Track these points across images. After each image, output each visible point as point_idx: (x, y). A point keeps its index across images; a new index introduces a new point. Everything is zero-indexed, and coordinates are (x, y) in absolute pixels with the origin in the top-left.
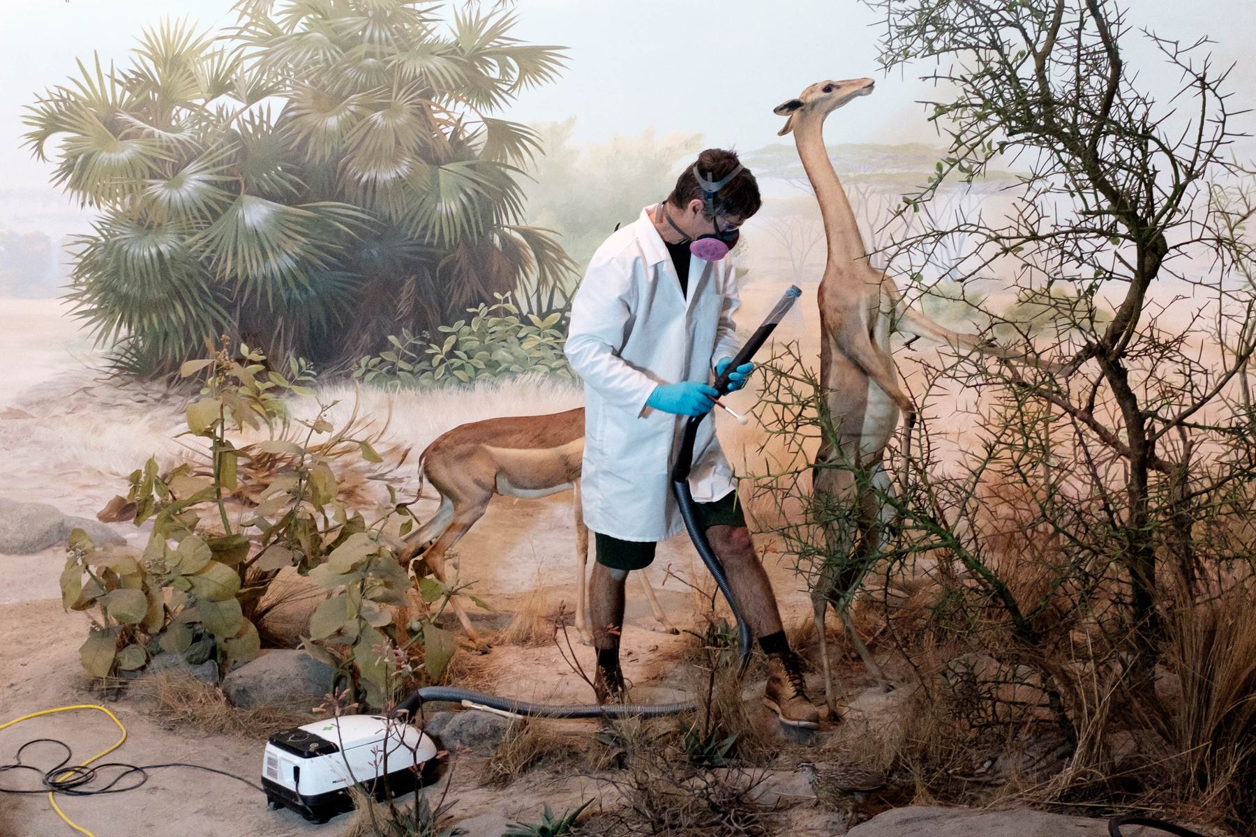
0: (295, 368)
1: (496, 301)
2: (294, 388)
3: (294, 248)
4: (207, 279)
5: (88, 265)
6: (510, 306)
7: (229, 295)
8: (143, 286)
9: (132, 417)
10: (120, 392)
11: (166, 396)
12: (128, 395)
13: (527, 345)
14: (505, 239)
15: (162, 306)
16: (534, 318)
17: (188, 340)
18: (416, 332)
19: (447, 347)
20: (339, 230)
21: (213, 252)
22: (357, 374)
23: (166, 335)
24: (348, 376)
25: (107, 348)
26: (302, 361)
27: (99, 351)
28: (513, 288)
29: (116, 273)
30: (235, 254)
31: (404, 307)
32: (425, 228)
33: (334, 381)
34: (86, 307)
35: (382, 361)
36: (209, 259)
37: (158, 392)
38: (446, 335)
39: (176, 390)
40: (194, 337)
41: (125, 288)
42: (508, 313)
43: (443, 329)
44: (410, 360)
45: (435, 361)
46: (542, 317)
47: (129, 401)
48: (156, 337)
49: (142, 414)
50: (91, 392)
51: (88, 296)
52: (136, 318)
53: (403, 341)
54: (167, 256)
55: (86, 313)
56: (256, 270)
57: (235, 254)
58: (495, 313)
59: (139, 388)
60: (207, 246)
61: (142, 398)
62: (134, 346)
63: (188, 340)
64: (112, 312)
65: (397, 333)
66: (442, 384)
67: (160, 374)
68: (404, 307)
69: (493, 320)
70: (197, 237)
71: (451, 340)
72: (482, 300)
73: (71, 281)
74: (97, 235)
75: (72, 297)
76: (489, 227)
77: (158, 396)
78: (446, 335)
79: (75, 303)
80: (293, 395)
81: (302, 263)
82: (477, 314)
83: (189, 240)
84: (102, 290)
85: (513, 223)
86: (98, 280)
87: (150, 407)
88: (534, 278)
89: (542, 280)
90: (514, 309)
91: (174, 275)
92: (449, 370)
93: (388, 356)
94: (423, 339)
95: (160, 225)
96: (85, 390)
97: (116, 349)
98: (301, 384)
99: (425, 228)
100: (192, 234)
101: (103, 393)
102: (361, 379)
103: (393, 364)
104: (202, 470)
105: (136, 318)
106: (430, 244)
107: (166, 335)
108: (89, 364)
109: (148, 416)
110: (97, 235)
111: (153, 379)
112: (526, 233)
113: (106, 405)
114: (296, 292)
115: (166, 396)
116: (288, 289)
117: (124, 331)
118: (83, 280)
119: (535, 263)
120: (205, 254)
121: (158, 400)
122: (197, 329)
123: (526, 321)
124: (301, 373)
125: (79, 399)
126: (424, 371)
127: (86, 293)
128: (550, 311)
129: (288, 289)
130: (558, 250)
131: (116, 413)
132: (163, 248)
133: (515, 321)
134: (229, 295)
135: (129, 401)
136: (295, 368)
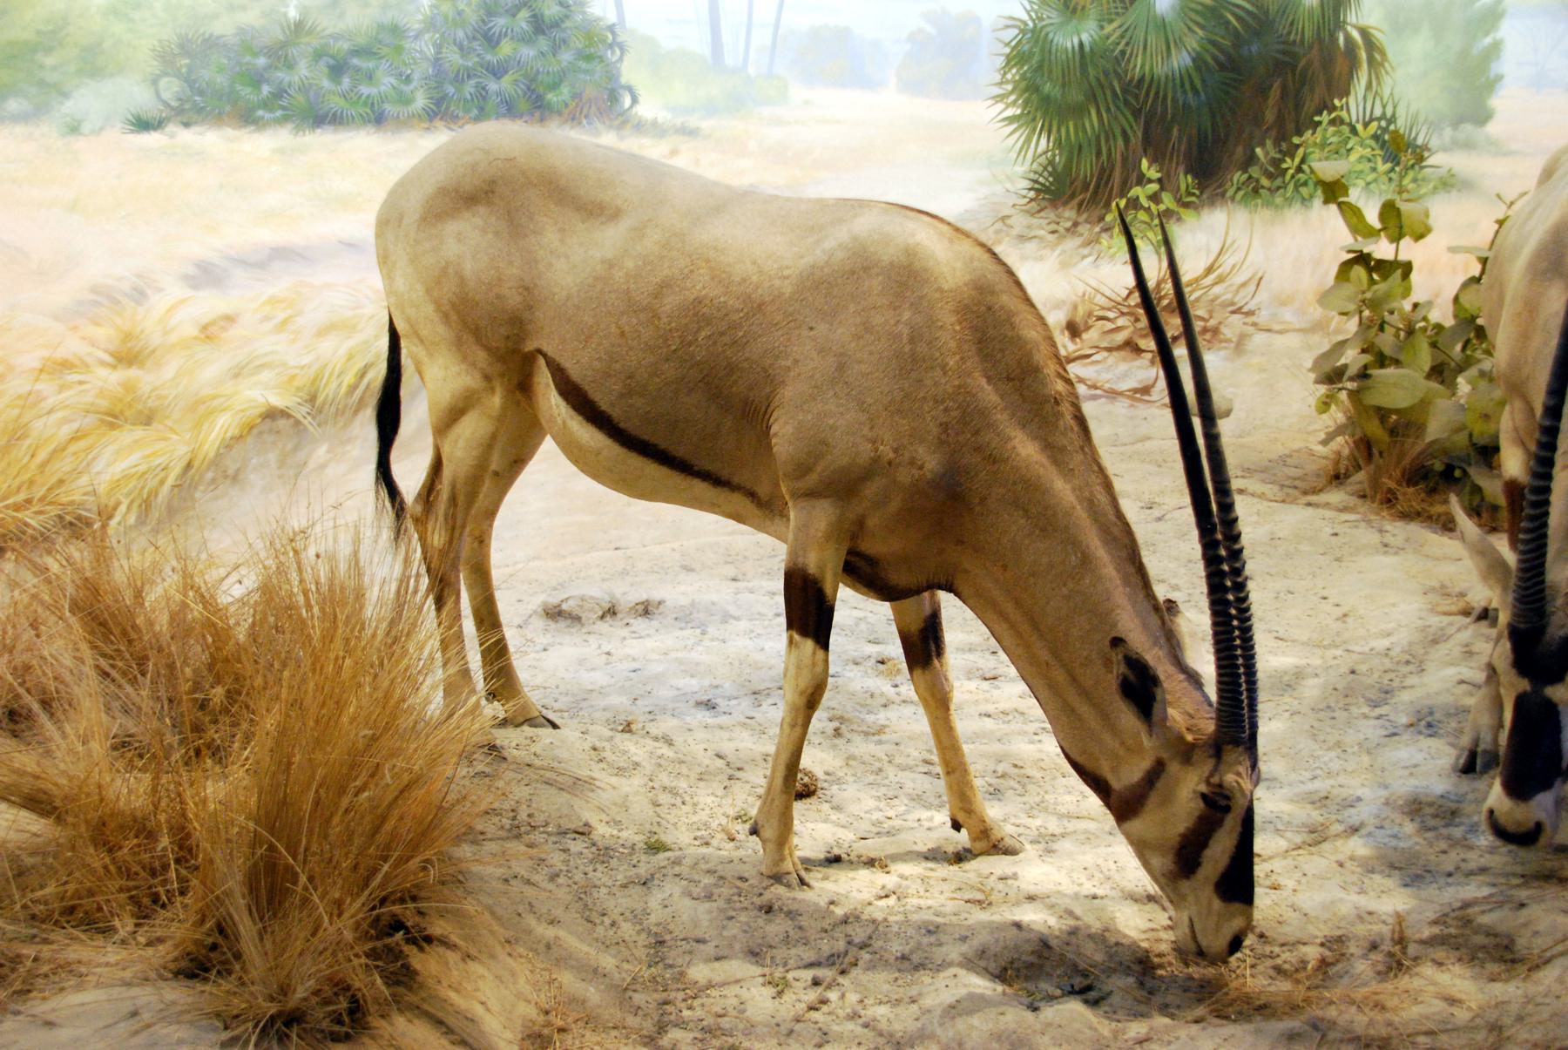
0: (1183, 187)
1: (1335, 108)
2: (1181, 210)
3: (1192, 43)
4: (1120, 78)
5: (1017, 57)
6: (1344, 114)
7: (1136, 97)
8: (1063, 85)
9: (1044, 252)
10: (1035, 221)
11: (1076, 224)
12: (1040, 225)
13: (1353, 157)
14: (1348, 38)
15: (1078, 111)
16: (1359, 127)
17: (1099, 153)
18: (1277, 143)
19: (1297, 160)
20: (1228, 22)
21: (1127, 44)
22: (1229, 194)
23: (1080, 147)
24: (1223, 195)
25: (1026, 167)
26: (1189, 178)
27: (1020, 169)
28: (1347, 93)
29: (1040, 67)
30: (1145, 48)
31: (1270, 116)
32: (1292, 24)
33: (1212, 203)
34: (1010, 112)
35: (1250, 177)
36: (1123, 53)
37: (1068, 219)
38: (1298, 146)
39: (1085, 216)
40: (1104, 150)
41: (1047, 88)
42: (1342, 122)
43: (1296, 140)
44: (1270, 176)
45: (1288, 177)
46: (1366, 125)
47: (1042, 233)
48: (1071, 152)
49: (1053, 247)
50: (1008, 222)
51: (1013, 97)
52: (1055, 129)
53: (1267, 154)
54: (1087, 49)
55: (1010, 120)
56: (1160, 70)
57: (1145, 48)
58: (1332, 122)
59: (1052, 216)
60: (1122, 37)
61: (1053, 227)
62: (1051, 162)
63: (1099, 153)
64: (1034, 119)
65: (1262, 145)
66: (1289, 201)
67: (1072, 196)
68: (1270, 116)
69: (1332, 129)
70: (1115, 25)
71: (1301, 152)
72: (1325, 107)
73: (998, 78)
74: (1025, 17)
75: (999, 98)
76: (1339, 24)
77: (1069, 224)
78: (1298, 146)
79: (1001, 106)
80: (1179, 219)
81: (1198, 60)
82: (1320, 123)
83: (1109, 28)
84: (1026, 90)
85: (1354, 21)
86: (1023, 77)
87: (1063, 237)
88: (1363, 82)
89: (1369, 86)
90: (1347, 120)
91: (1092, 72)
92: (1296, 187)
93: (1255, 171)
94: (1280, 151)
95: (1083, 8)
96: (1003, 219)
97: (1035, 166)
98: (1186, 205)
99: (1292, 24)
100: (1111, 21)
101: (1020, 222)
102: (1233, 199)
103: (1257, 181)
104: (1101, 313)
105: (1055, 129)
106: (1294, 42)
107: (1080, 147)
108: (1009, 186)
109: (1057, 252)
110: (1025, 17)
111: (1065, 204)
112: (1364, 33)
113: (1022, 238)
114: (1190, 95)
115: (1076, 224)
116: (1185, 92)
117: (1043, 141)
118: (1009, 76)
119: (1365, 65)
120: (1120, 47)
121: (1068, 230)
122: (1107, 141)
123: (1354, 131)
124: (1190, 194)
125: (997, 232)
126: (1279, 188)
127: (1011, 93)
128: (1372, 120)
129: (1185, 92)
130: (1383, 53)
131: (1031, 247)
132: (1085, 37)
133: (1345, 129)
134: (1136, 97)
135: (1042, 233)
136: (1183, 187)
